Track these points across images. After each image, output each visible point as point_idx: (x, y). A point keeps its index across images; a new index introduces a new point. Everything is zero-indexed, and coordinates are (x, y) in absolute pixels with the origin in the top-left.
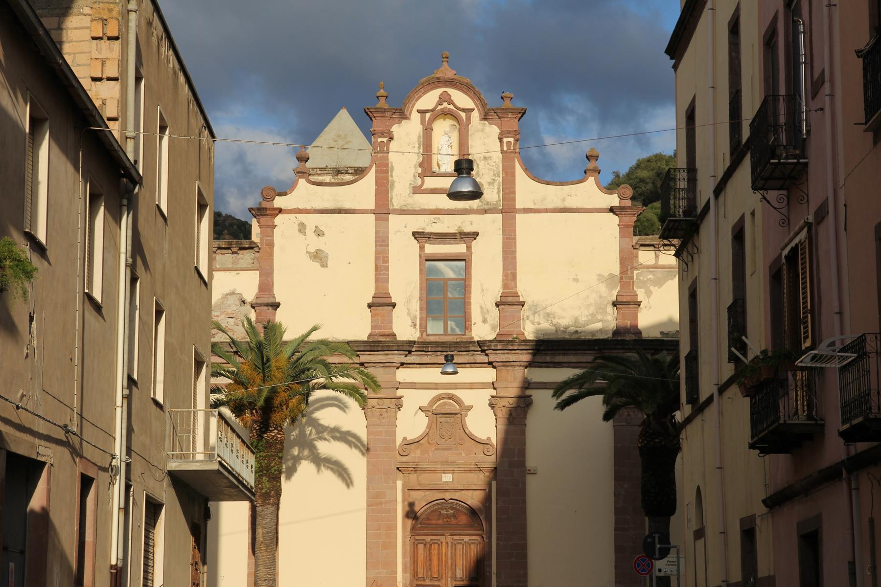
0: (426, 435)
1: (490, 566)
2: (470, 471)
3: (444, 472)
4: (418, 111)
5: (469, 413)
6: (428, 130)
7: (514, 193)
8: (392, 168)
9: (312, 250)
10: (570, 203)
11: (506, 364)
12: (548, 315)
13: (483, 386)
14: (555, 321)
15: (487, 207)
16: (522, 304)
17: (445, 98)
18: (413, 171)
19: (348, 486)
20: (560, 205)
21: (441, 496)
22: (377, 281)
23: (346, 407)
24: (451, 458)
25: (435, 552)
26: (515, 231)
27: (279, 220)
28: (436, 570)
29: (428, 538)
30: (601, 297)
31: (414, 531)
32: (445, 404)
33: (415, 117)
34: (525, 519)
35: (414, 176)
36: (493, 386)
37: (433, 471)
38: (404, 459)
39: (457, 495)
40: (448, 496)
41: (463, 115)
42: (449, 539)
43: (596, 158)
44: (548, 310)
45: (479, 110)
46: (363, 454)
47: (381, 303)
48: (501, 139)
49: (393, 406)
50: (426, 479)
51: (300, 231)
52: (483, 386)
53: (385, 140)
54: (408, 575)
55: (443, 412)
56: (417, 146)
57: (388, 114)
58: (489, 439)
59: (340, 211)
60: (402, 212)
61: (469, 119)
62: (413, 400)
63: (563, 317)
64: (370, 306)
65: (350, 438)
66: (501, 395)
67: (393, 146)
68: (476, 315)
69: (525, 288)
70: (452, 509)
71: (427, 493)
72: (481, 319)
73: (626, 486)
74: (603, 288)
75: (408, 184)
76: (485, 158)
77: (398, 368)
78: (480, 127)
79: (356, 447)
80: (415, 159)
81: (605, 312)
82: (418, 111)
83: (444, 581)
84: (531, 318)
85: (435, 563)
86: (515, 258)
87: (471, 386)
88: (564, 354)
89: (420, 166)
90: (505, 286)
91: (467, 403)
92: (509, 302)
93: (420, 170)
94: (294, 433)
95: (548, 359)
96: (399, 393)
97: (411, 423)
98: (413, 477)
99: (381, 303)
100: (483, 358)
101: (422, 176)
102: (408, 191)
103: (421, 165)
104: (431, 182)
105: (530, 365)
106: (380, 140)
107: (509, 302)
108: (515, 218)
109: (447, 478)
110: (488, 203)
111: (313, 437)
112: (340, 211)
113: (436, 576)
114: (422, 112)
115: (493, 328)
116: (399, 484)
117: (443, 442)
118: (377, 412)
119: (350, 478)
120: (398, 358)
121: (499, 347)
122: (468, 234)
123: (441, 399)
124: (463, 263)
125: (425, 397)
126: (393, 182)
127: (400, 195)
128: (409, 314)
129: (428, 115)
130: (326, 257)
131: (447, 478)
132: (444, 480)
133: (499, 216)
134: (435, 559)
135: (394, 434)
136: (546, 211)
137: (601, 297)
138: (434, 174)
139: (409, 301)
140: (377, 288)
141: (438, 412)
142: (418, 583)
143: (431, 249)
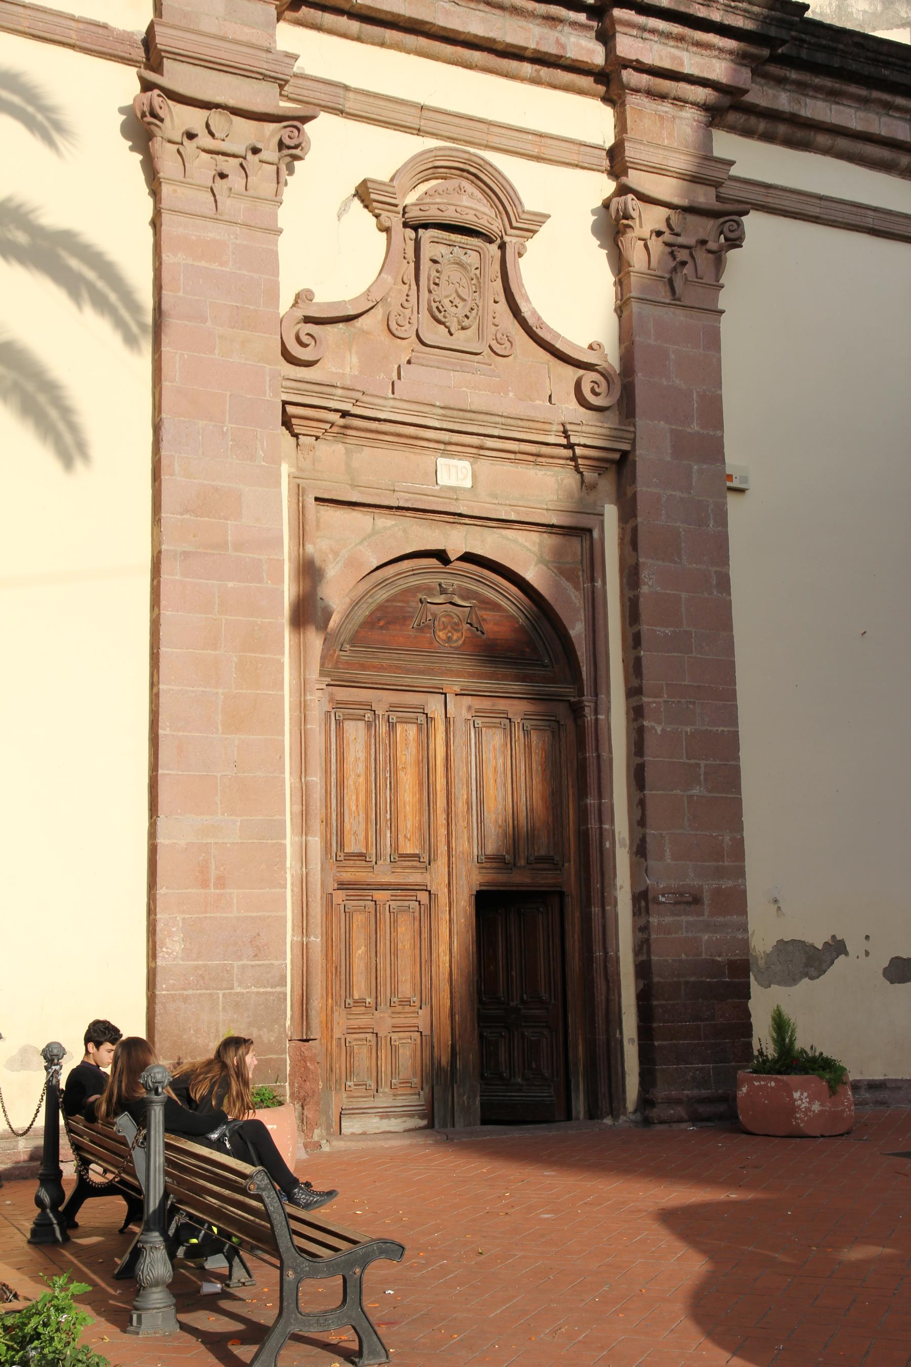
3: (447, 449)
5: (533, 245)
19: (67, 461)
21: (430, 536)
23: (59, 127)
24: (477, 400)
28: (409, 821)
29: (382, 700)
39: (487, 543)
42: (460, 708)
46: (130, 340)
49: (270, 153)
50: (377, 468)
54: (316, 842)
55: (450, 215)
62: (343, 153)
65: (74, 263)
71: (385, 521)
79: (101, 304)
87: (541, 148)
88: (833, 95)
91: (531, 202)
95: (783, 101)
105: (727, 109)
109: (455, 473)
113: (409, 848)
117: (435, 334)
119: (73, 428)
131: (455, 473)
132: (444, 479)
134: (408, 781)
141: (432, 214)
142: (347, 876)
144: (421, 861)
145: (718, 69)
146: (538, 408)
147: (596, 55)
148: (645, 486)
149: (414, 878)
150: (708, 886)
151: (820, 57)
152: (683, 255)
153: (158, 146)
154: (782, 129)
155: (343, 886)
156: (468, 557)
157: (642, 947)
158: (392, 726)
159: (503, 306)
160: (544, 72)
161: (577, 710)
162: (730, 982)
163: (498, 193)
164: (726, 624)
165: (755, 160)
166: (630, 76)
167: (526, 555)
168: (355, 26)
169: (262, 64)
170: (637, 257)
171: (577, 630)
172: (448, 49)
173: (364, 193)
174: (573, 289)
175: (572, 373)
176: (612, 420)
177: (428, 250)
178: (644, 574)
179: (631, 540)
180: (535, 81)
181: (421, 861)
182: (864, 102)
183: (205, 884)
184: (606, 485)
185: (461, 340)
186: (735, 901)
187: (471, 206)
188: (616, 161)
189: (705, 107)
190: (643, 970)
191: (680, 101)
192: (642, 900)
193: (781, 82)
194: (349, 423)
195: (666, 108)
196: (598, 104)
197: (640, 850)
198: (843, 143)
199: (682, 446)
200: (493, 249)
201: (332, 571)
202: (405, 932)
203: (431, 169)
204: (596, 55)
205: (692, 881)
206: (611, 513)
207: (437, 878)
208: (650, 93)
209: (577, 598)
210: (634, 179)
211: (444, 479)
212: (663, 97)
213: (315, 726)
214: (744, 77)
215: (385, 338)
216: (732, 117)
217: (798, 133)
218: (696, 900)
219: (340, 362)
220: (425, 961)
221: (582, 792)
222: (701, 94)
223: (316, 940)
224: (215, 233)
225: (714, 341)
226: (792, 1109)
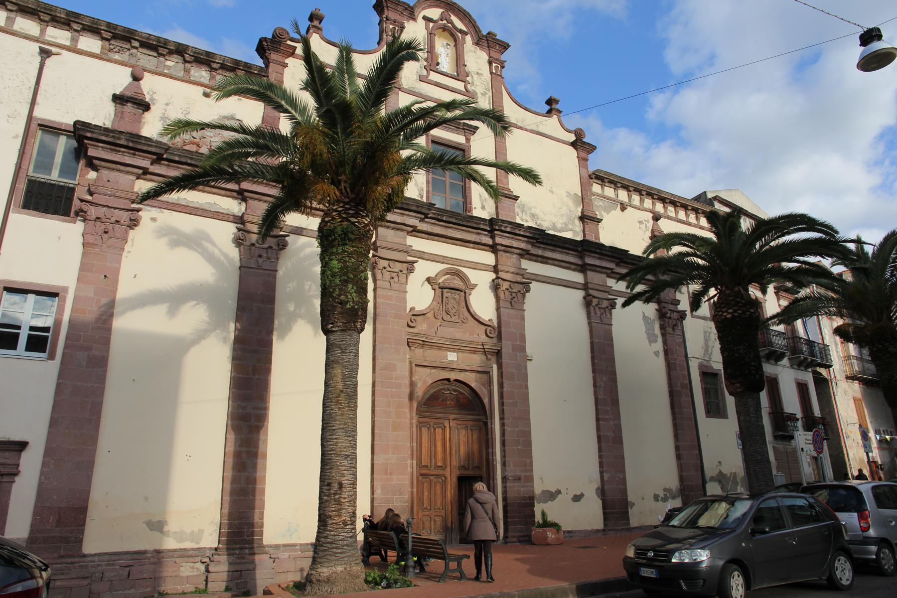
3: (450, 350)
4: (425, 18)
11: (508, 249)
14: (539, 222)
16: (516, 198)
20: (535, 129)
24: (459, 336)
25: (439, 437)
30: (570, 211)
31: (419, 412)
33: (421, 22)
37: (439, 347)
38: (411, 330)
39: (461, 376)
40: (453, 376)
42: (453, 424)
43: (557, 102)
44: (533, 211)
45: (472, 36)
48: (490, 63)
50: (431, 355)
54: (415, 462)
55: (452, 286)
57: (400, 8)
62: (424, 269)
71: (433, 371)
72: (480, 206)
74: (571, 204)
75: (415, 72)
81: (574, 224)
82: (425, 18)
83: (448, 469)
84: (520, 214)
87: (475, 266)
88: (553, 251)
94: (291, 285)
95: (540, 252)
98: (419, 351)
100: (488, 240)
102: (416, 77)
104: (433, 76)
106: (391, 27)
109: (452, 356)
111: (312, 293)
117: (447, 318)
118: (387, 275)
121: (508, 230)
129: (431, 25)
132: (449, 358)
134: (439, 444)
137: (570, 211)
141: (447, 285)
144: (443, 468)
145: (523, 245)
146: (475, 338)
147: (490, 242)
148: (505, 360)
149: (441, 472)
150: (523, 474)
151: (549, 242)
152: (514, 295)
153: (376, 270)
154: (540, 259)
155: (421, 475)
156: (456, 380)
157: (505, 492)
158: (435, 429)
159: (465, 309)
160: (476, 246)
161: (486, 424)
162: (529, 502)
163: (464, 278)
164: (528, 399)
165: (531, 267)
166: (499, 247)
167: (471, 379)
168: (426, 236)
169: (404, 249)
170: (502, 296)
171: (486, 401)
172: (451, 241)
173: (428, 280)
174: (483, 304)
175: (484, 328)
176: (495, 341)
177: (445, 295)
178: (505, 385)
179: (501, 375)
180: (473, 248)
181: (443, 468)
182: (561, 252)
183: (386, 474)
184: (494, 359)
185: (454, 319)
186: (530, 479)
187: (457, 283)
188: (496, 269)
189: (519, 254)
190: (505, 499)
191: (512, 253)
192: (504, 479)
193: (539, 247)
194: (424, 344)
195: (509, 255)
196: (490, 253)
197: (504, 464)
198: (556, 262)
200: (463, 294)
201: (420, 384)
202: (438, 488)
203: (446, 272)
204: (490, 241)
205: (518, 473)
206: (495, 367)
207: (447, 473)
208: (504, 251)
209: (486, 392)
210: (501, 275)
211: (449, 358)
212: (508, 252)
213: (414, 429)
214: (528, 247)
215: (434, 319)
216: (526, 256)
217: (544, 260)
218: (520, 479)
219: (422, 327)
220: (444, 497)
221: (487, 448)
222: (518, 251)
223: (415, 490)
224: (390, 293)
225: (523, 318)
226: (547, 537)
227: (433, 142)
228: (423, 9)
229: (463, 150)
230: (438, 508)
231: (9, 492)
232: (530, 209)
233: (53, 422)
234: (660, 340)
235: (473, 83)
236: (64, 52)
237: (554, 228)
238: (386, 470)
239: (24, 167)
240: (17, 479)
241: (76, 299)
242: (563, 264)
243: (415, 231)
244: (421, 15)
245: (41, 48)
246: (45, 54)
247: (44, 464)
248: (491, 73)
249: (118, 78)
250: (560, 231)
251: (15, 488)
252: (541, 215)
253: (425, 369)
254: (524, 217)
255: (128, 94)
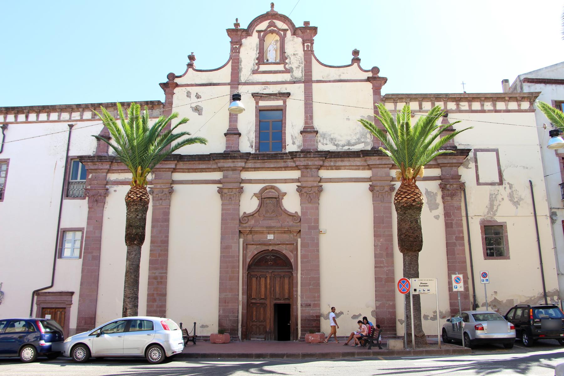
0: (258, 211)
1: (297, 291)
2: (285, 232)
6: (262, 41)
7: (311, 72)
8: (241, 61)
9: (194, 105)
10: (342, 78)
11: (306, 167)
12: (332, 139)
13: (293, 181)
15: (295, 80)
16: (317, 132)
17: (272, 25)
18: (253, 62)
20: (338, 78)
22: (230, 121)
26: (312, 92)
27: (176, 90)
32: (270, 192)
33: (255, 34)
34: (319, 262)
35: (254, 65)
36: (298, 180)
37: (262, 233)
39: (276, 248)
40: (271, 248)
41: (282, 33)
47: (233, 133)
48: (303, 44)
50: (257, 237)
51: (188, 96)
52: (293, 181)
53: (237, 46)
56: (256, 49)
58: (296, 213)
59: (210, 84)
60: (246, 84)
61: (285, 35)
62: (251, 190)
63: (341, 141)
64: (226, 135)
66: (304, 186)
67: (242, 49)
68: (288, 140)
69: (317, 124)
70: (273, 256)
73: (381, 240)
75: (250, 69)
76: (294, 54)
77: (241, 171)
78: (291, 39)
80: (254, 54)
81: (366, 137)
84: (322, 141)
85: (263, 289)
86: (312, 107)
87: (285, 181)
88: (342, 161)
89: (257, 59)
90: (306, 123)
92: (309, 131)
93: (257, 61)
96: (242, 185)
97: (249, 204)
98: (250, 237)
99: (233, 133)
101: (258, 64)
103: (257, 59)
104: (263, 68)
107: (309, 131)
108: (312, 86)
109: (270, 237)
110: (296, 78)
112: (210, 84)
113: (263, 297)
114: (259, 32)
115: (299, 147)
116: (241, 240)
120: (240, 164)
122: (284, 94)
123: (267, 189)
124: (281, 112)
125: (257, 188)
126: (242, 68)
127: (245, 74)
128: (249, 140)
129: (262, 34)
130: (202, 109)
131: (270, 237)
132: (268, 238)
133: (303, 85)
135: (238, 210)
136: (330, 81)
138: (264, 64)
139: (249, 132)
140: (230, 126)
143: (262, 103)
144: (265, 299)
150: (312, 303)
158: (260, 278)
181: (265, 299)
199: (310, 228)
205: (309, 302)
207: (268, 302)
218: (310, 305)
222: (314, 167)
226: (309, 339)
227: (260, 110)
228: (256, 26)
229: (282, 110)
230: (262, 321)
231: (69, 311)
232: (330, 135)
233: (82, 284)
234: (441, 207)
235: (290, 63)
236: (78, 122)
237: (349, 144)
238: (225, 301)
239: (67, 179)
240: (72, 306)
241: (87, 232)
242: (353, 167)
243: (245, 169)
244: (255, 31)
245: (69, 125)
246: (71, 126)
247: (79, 301)
248: (304, 50)
249: (97, 128)
250: (353, 145)
251: (71, 309)
252: (338, 138)
253: (253, 246)
254: (325, 142)
255: (102, 134)
